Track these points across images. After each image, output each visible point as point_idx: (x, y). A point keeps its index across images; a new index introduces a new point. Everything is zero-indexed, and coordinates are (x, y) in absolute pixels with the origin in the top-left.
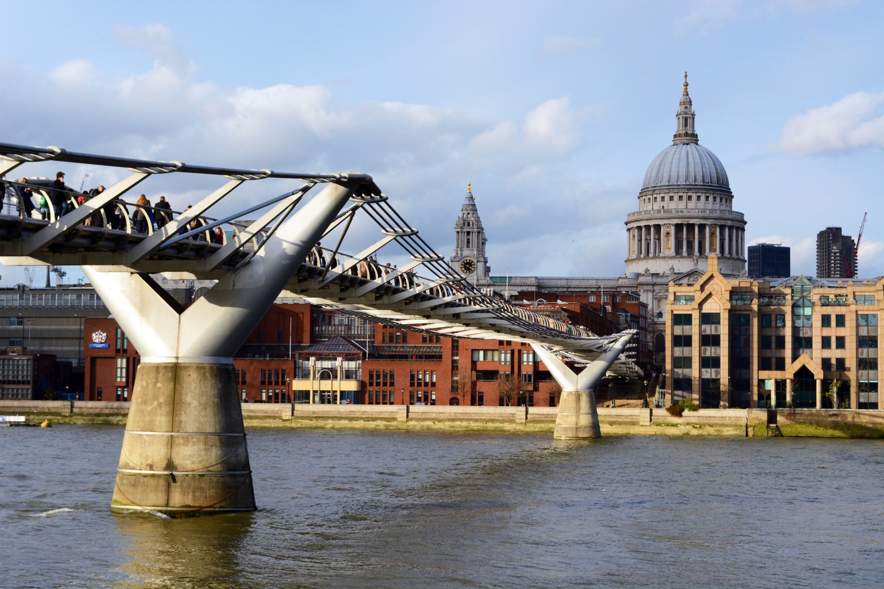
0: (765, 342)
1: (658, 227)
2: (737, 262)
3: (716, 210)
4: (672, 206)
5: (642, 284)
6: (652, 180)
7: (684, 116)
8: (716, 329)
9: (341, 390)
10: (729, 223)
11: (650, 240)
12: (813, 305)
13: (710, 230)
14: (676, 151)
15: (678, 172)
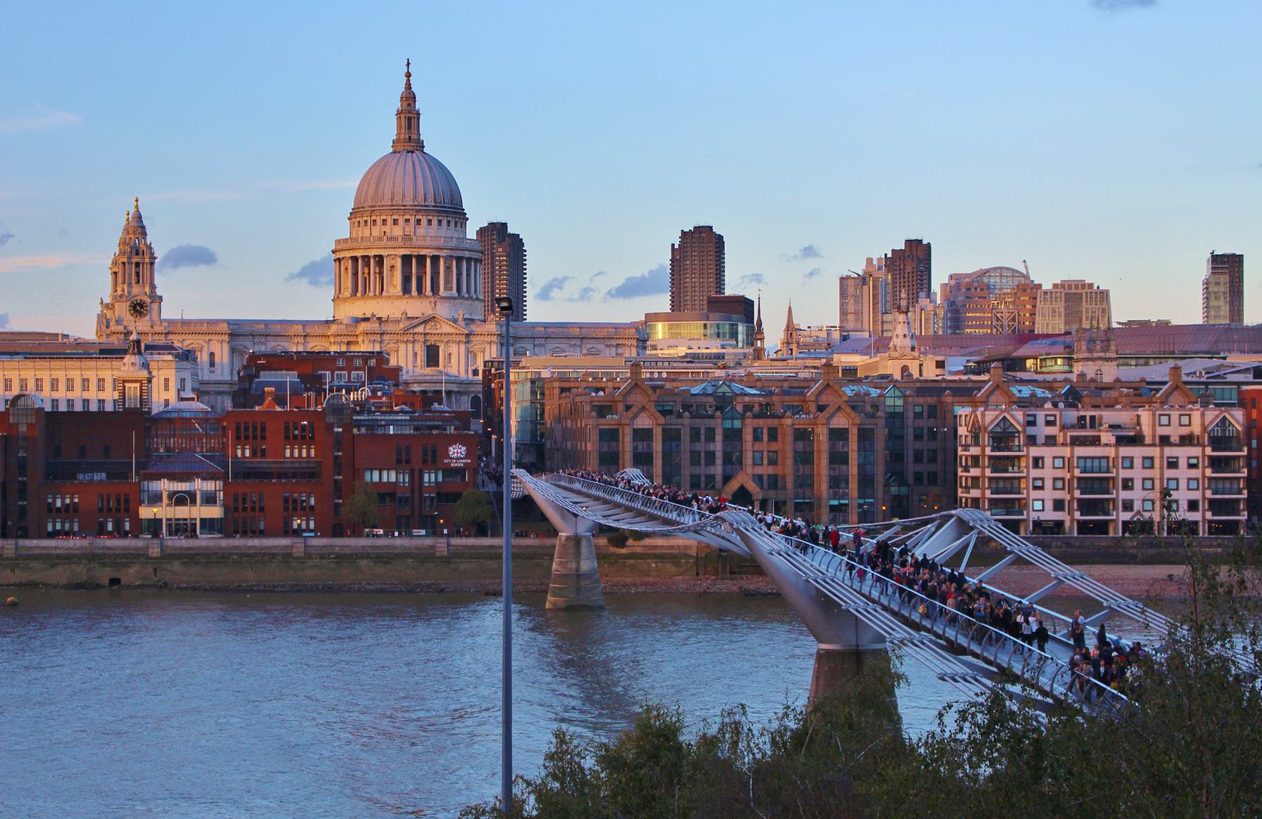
0: (695, 459)
1: (380, 260)
2: (476, 303)
3: (452, 238)
4: (398, 231)
5: (367, 334)
6: (369, 197)
7: (407, 115)
8: (649, 446)
9: (202, 517)
10: (467, 254)
11: (369, 274)
12: (743, 417)
13: (445, 263)
14: (399, 161)
15: (404, 189)
